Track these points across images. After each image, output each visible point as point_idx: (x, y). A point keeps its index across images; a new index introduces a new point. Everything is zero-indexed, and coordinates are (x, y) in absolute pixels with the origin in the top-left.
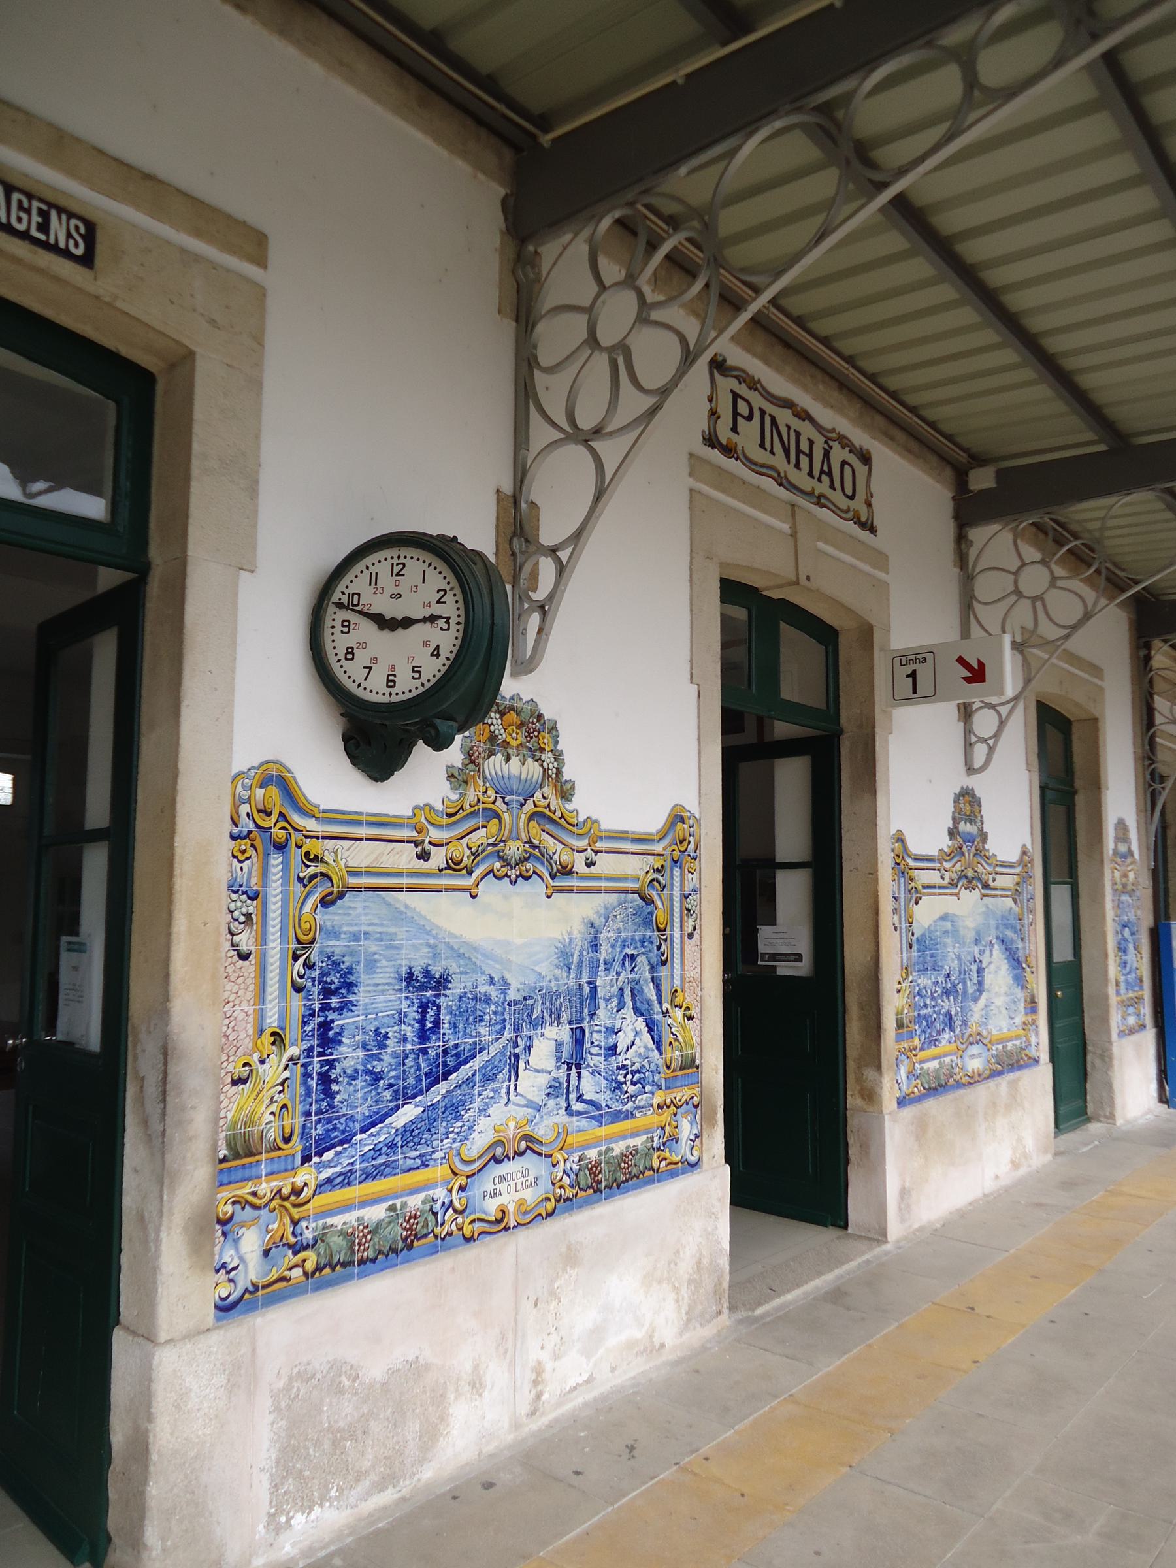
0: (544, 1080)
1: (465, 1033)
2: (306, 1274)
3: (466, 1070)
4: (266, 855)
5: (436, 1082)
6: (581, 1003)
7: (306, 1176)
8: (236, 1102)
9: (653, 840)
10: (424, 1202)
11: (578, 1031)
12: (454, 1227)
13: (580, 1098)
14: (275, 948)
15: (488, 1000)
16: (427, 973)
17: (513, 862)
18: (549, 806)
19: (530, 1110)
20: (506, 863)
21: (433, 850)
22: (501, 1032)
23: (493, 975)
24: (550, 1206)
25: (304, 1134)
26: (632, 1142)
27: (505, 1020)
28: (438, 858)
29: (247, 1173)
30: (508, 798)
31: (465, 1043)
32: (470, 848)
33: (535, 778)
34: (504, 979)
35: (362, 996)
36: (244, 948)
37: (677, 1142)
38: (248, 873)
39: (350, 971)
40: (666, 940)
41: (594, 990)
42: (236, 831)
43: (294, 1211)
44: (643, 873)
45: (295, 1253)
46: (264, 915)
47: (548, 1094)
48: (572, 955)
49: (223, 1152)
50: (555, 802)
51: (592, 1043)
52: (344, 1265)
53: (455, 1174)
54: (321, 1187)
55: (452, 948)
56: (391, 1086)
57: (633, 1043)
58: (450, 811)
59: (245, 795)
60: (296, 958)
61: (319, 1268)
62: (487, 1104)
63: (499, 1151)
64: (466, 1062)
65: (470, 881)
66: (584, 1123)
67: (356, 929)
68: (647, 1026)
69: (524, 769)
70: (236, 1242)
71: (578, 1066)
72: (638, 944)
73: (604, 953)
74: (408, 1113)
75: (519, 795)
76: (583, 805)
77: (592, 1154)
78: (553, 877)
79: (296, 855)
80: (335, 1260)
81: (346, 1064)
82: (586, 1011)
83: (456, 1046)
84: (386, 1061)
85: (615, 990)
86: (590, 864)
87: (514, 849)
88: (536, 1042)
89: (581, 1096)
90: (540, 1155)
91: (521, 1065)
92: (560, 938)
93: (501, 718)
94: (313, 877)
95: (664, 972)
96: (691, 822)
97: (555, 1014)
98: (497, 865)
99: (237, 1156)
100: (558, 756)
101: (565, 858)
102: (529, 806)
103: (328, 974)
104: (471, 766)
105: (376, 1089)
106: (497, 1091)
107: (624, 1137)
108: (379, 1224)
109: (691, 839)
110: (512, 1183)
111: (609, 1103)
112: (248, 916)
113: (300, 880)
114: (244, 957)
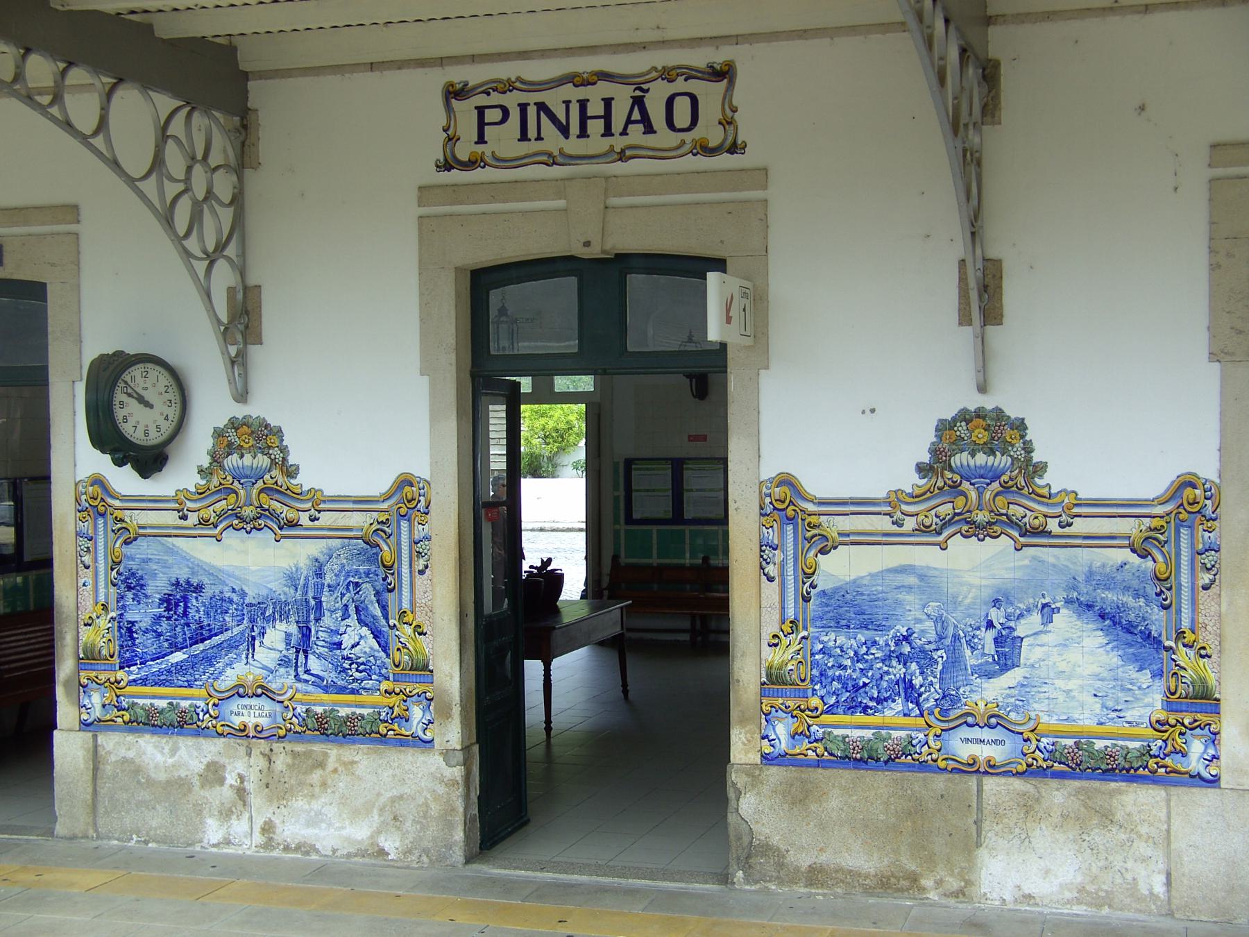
0: (277, 655)
1: (215, 619)
2: (124, 722)
3: (216, 640)
4: (96, 519)
5: (196, 643)
6: (308, 611)
7: (120, 674)
9: (378, 501)
10: (190, 706)
11: (305, 629)
12: (210, 724)
13: (307, 672)
15: (231, 601)
16: (188, 583)
17: (248, 520)
18: (276, 482)
19: (265, 671)
20: (242, 519)
21: (190, 514)
22: (240, 623)
23: (234, 587)
24: (282, 732)
25: (119, 655)
26: (358, 711)
27: (244, 614)
28: (193, 519)
29: (93, 667)
30: (242, 481)
31: (216, 626)
32: (214, 512)
33: (264, 466)
34: (242, 590)
36: (87, 563)
37: (407, 721)
38: (86, 527)
39: (142, 578)
40: (393, 574)
41: (319, 604)
42: (80, 508)
43: (117, 690)
44: (367, 525)
45: (118, 711)
46: (96, 548)
47: (279, 665)
48: (299, 579)
49: (81, 656)
51: (318, 638)
52: (144, 724)
53: (211, 696)
54: (131, 683)
55: (204, 569)
56: (167, 640)
57: (358, 644)
58: (199, 491)
59: (84, 490)
60: (112, 569)
61: (130, 721)
62: (231, 661)
63: (241, 690)
64: (216, 635)
65: (217, 531)
66: (311, 688)
67: (144, 556)
68: (372, 633)
69: (255, 461)
70: (90, 696)
71: (305, 652)
72: (363, 575)
73: (329, 579)
75: (252, 478)
76: (305, 480)
77: (319, 710)
78: (281, 528)
79: (110, 519)
80: (140, 720)
81: (141, 624)
82: (312, 616)
83: (209, 625)
85: (339, 605)
86: (313, 519)
87: (248, 512)
88: (268, 631)
89: (308, 670)
90: (274, 700)
91: (257, 643)
92: (288, 568)
93: (236, 431)
94: (119, 530)
95: (391, 598)
96: (421, 485)
98: (236, 522)
99: (88, 659)
100: (284, 450)
101: (292, 515)
102: (260, 483)
103: (129, 579)
104: (215, 464)
105: (159, 640)
106: (239, 655)
107: (349, 706)
108: (163, 710)
109: (421, 498)
110: (252, 712)
111: (335, 680)
112: (88, 548)
113: (113, 531)
114: (87, 567)
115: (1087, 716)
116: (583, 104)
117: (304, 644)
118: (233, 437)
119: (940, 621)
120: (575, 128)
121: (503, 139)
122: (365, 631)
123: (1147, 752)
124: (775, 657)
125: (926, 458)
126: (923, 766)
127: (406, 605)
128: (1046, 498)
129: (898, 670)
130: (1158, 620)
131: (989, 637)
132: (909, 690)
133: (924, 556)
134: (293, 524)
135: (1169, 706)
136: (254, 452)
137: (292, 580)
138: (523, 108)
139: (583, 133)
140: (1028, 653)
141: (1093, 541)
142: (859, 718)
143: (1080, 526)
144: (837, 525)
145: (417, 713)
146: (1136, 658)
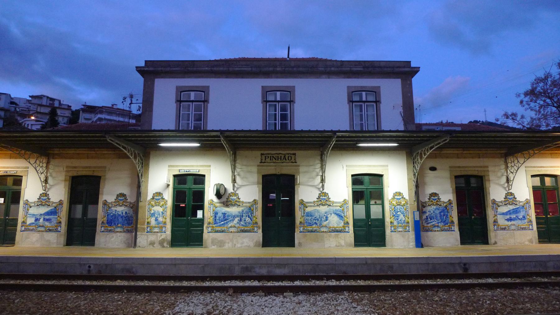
7: (214, 225)
8: (209, 220)
14: (212, 211)
31: (228, 218)
35: (218, 214)
38: (209, 206)
41: (243, 215)
50: (238, 200)
73: (244, 212)
74: (222, 223)
76: (241, 200)
77: (242, 229)
84: (220, 219)
87: (233, 204)
97: (238, 217)
100: (238, 196)
115: (335, 226)
116: (278, 157)
117: (241, 220)
118: (231, 194)
119: (319, 215)
120: (277, 159)
121: (268, 160)
122: (249, 219)
123: (342, 230)
124: (301, 220)
125: (318, 197)
126: (318, 232)
127: (255, 215)
128: (330, 201)
129: (315, 221)
130: (343, 215)
131: (325, 217)
132: (316, 223)
133: (318, 208)
134: (239, 205)
135: (344, 224)
136: (234, 196)
137: (239, 212)
138: (271, 157)
139: (278, 160)
140: (329, 219)
141: (336, 206)
142: (311, 227)
143: (334, 205)
144: (308, 205)
145: (256, 229)
146: (340, 219)
